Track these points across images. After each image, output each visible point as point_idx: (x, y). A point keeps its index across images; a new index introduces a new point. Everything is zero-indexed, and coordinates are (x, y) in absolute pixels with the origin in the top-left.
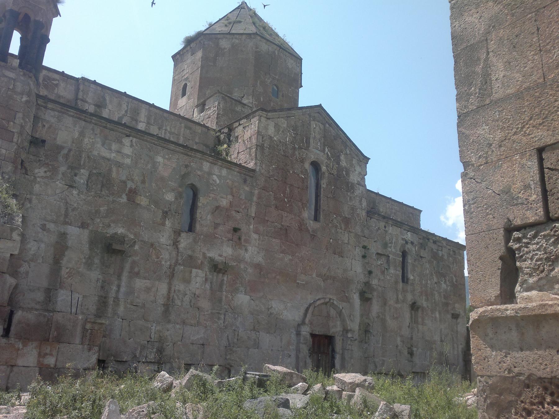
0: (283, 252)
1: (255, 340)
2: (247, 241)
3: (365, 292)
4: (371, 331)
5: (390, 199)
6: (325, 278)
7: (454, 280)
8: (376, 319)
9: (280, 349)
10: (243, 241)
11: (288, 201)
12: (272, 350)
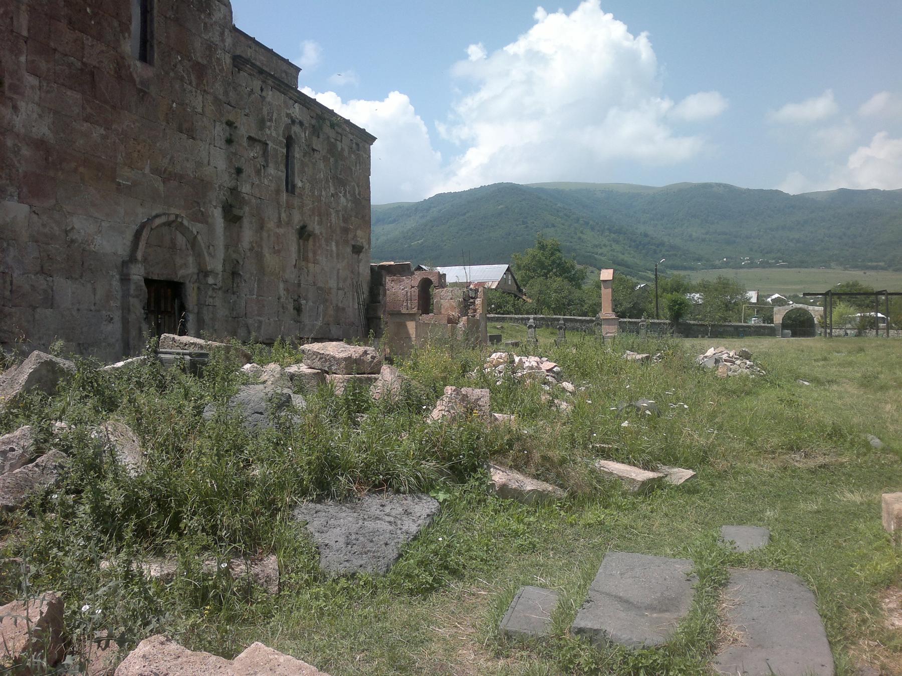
0: (87, 119)
1: (45, 291)
2: (15, 89)
3: (231, 206)
4: (241, 273)
5: (253, 40)
6: (167, 176)
7: (357, 193)
8: (248, 254)
9: (93, 308)
10: (6, 89)
11: (92, 12)
12: (78, 310)
